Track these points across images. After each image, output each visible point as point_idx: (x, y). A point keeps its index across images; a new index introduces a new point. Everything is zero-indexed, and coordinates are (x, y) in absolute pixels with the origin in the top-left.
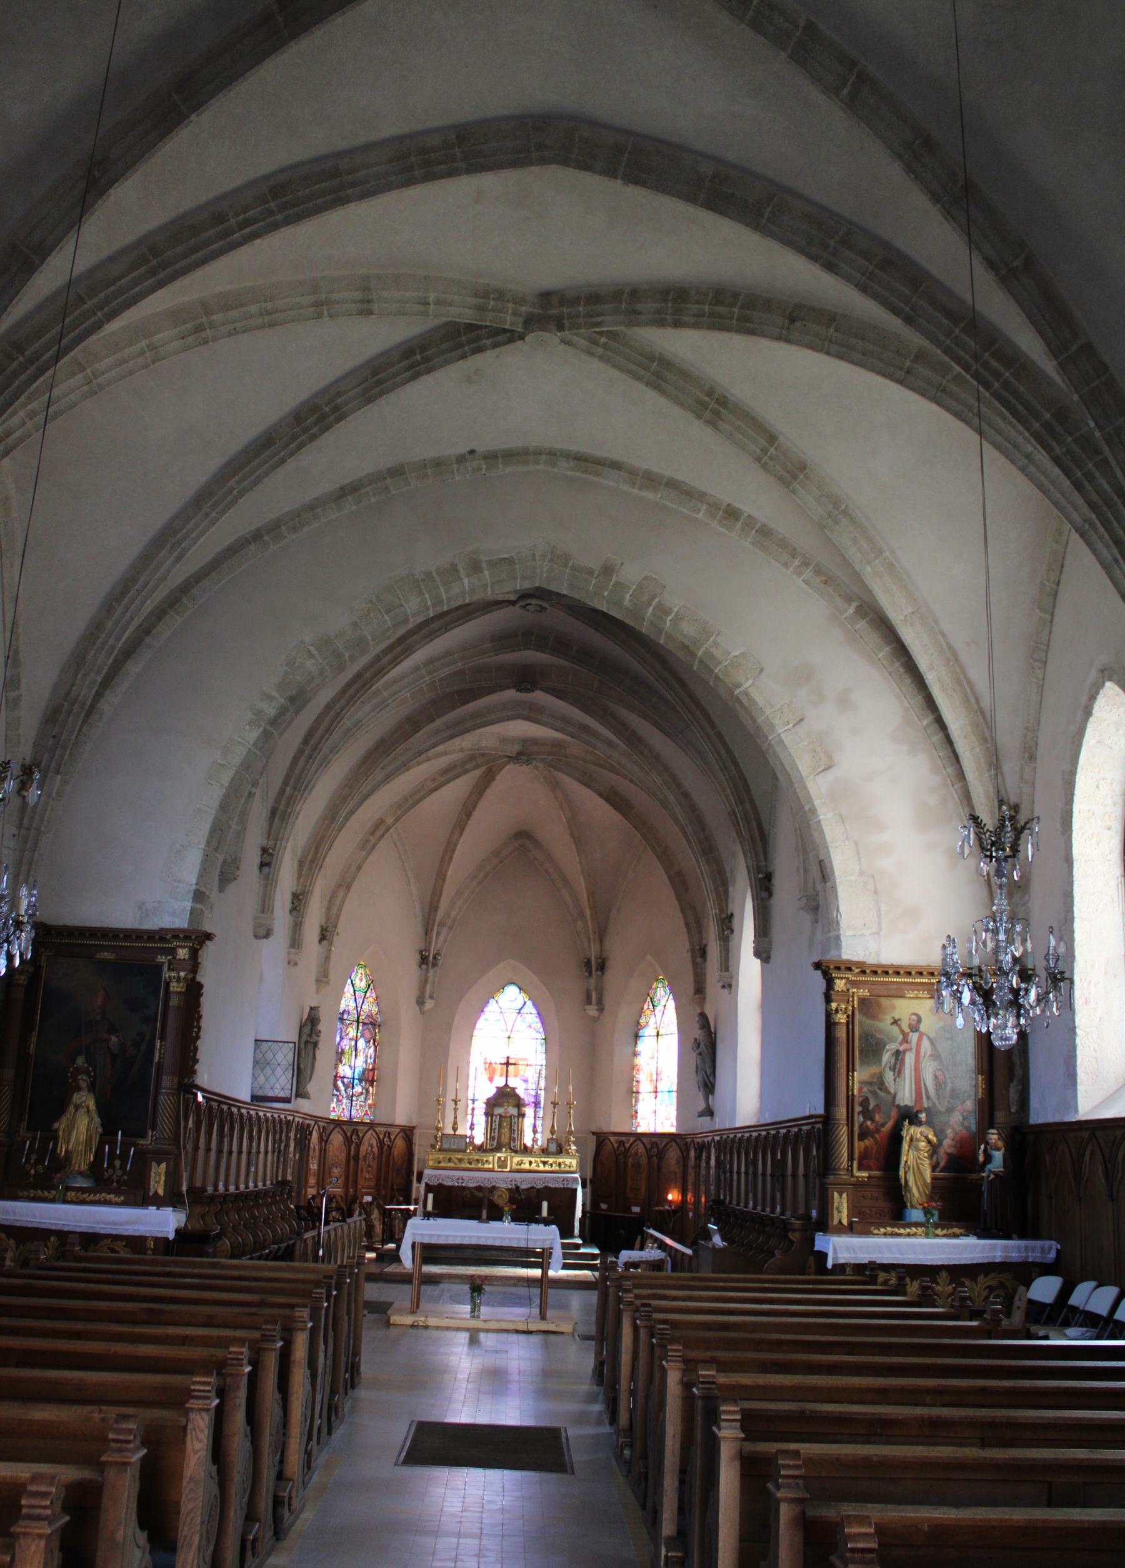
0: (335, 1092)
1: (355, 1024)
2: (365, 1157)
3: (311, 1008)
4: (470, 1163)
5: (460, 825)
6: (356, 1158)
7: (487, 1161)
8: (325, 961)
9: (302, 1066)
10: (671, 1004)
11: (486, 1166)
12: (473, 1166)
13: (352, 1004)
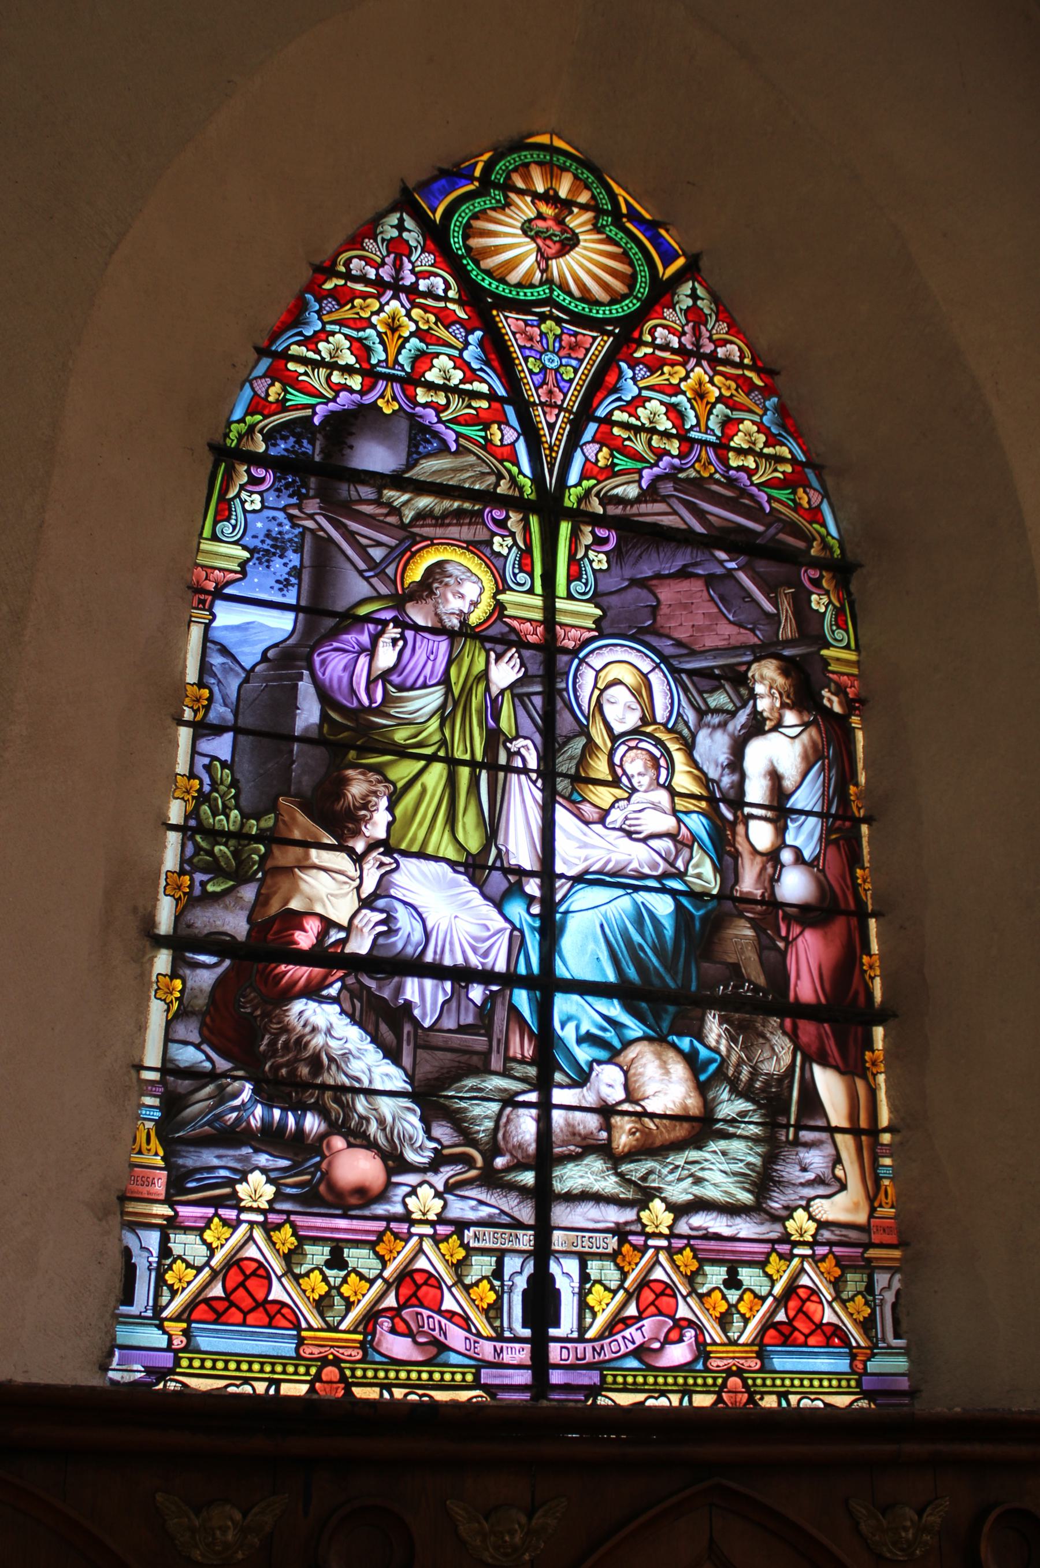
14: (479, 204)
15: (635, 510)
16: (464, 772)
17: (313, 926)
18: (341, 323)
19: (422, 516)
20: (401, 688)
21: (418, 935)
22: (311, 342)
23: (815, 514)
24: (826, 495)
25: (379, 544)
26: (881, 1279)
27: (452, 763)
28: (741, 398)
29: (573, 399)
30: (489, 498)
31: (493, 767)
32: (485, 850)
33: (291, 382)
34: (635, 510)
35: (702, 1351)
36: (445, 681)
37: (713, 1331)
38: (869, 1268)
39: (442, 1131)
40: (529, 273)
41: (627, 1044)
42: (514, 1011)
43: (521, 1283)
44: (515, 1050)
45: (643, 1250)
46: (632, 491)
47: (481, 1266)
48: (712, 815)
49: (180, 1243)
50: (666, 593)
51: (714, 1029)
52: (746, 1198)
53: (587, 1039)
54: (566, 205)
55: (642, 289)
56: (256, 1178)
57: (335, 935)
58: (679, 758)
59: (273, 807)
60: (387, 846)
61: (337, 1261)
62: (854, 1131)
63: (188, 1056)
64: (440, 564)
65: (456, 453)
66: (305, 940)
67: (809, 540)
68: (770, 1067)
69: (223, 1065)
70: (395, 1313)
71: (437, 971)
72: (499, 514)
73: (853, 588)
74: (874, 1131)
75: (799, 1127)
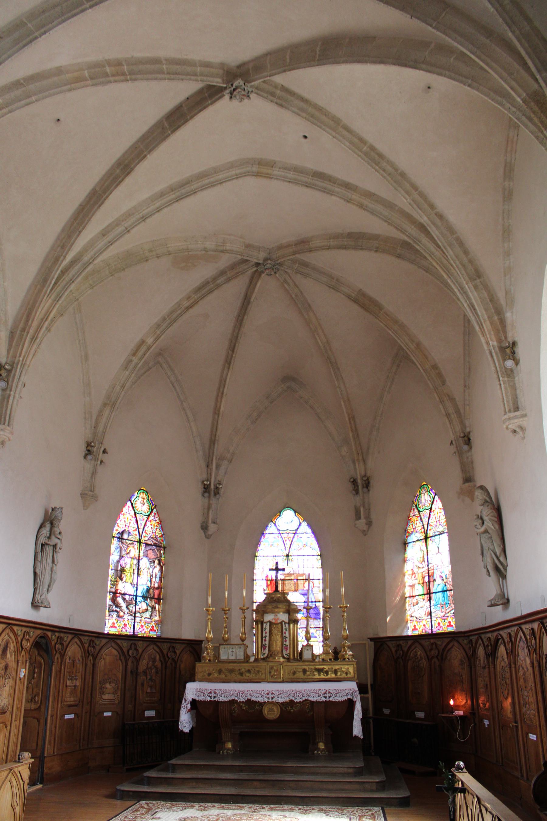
0: (114, 608)
1: (137, 544)
2: (145, 672)
3: (53, 510)
5: (228, 362)
6: (135, 673)
8: (92, 477)
9: (37, 571)
10: (438, 504)
13: (133, 526)
14: (136, 499)
23: (163, 541)
29: (142, 527)
30: (134, 541)
33: (118, 526)
35: (145, 632)
37: (146, 630)
38: (158, 624)
39: (128, 610)
50: (149, 552)
51: (148, 600)
54: (144, 499)
55: (150, 511)
59: (116, 578)
66: (119, 592)
67: (162, 544)
71: (128, 595)
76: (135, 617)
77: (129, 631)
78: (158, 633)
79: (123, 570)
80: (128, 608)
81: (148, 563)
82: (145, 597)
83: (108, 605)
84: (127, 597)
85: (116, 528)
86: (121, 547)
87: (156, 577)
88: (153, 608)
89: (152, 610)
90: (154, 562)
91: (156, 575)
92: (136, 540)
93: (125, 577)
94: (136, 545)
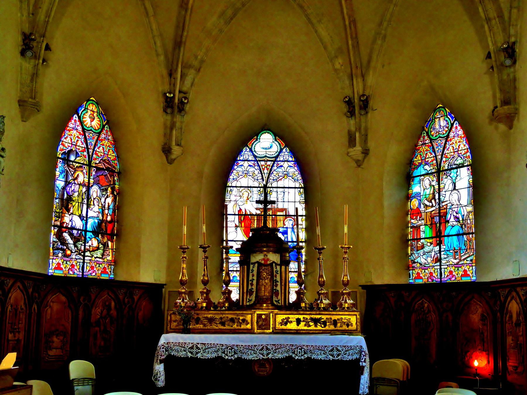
4: (223, 324)
7: (244, 320)
11: (243, 327)
12: (227, 327)
14: (85, 112)
15: (98, 165)
16: (80, 204)
17: (65, 224)
18: (69, 135)
19: (77, 167)
20: (74, 192)
21: (75, 225)
22: (66, 138)
24: (118, 161)
25: (72, 171)
26: (112, 266)
27: (78, 203)
28: (111, 146)
29: (92, 147)
31: (82, 203)
32: (81, 214)
34: (98, 165)
35: (96, 274)
36: (78, 191)
40: (89, 125)
41: (92, 238)
42: (82, 234)
43: (81, 266)
44: (82, 239)
45: (92, 262)
46: (98, 162)
47: (78, 264)
48: (102, 209)
49: (54, 261)
51: (100, 236)
52: (101, 257)
53: (89, 238)
54: (93, 112)
56: (60, 254)
57: (67, 225)
58: (100, 201)
60: (72, 214)
61: (66, 263)
62: (111, 249)
63: (55, 240)
64: (78, 174)
65: (80, 157)
66: (65, 225)
68: (104, 241)
69: (58, 241)
70: (71, 269)
71: (76, 229)
72: (84, 166)
73: (119, 176)
74: (113, 249)
75: (106, 248)
76: (84, 256)
77: (77, 273)
78: (111, 276)
79: (70, 199)
80: (75, 246)
81: (99, 191)
82: (96, 233)
83: (52, 242)
84: (75, 232)
85: (61, 147)
86: (67, 171)
87: (109, 209)
88: (105, 245)
89: (104, 248)
90: (106, 190)
91: (109, 206)
92: (85, 163)
93: (72, 208)
94: (86, 169)
